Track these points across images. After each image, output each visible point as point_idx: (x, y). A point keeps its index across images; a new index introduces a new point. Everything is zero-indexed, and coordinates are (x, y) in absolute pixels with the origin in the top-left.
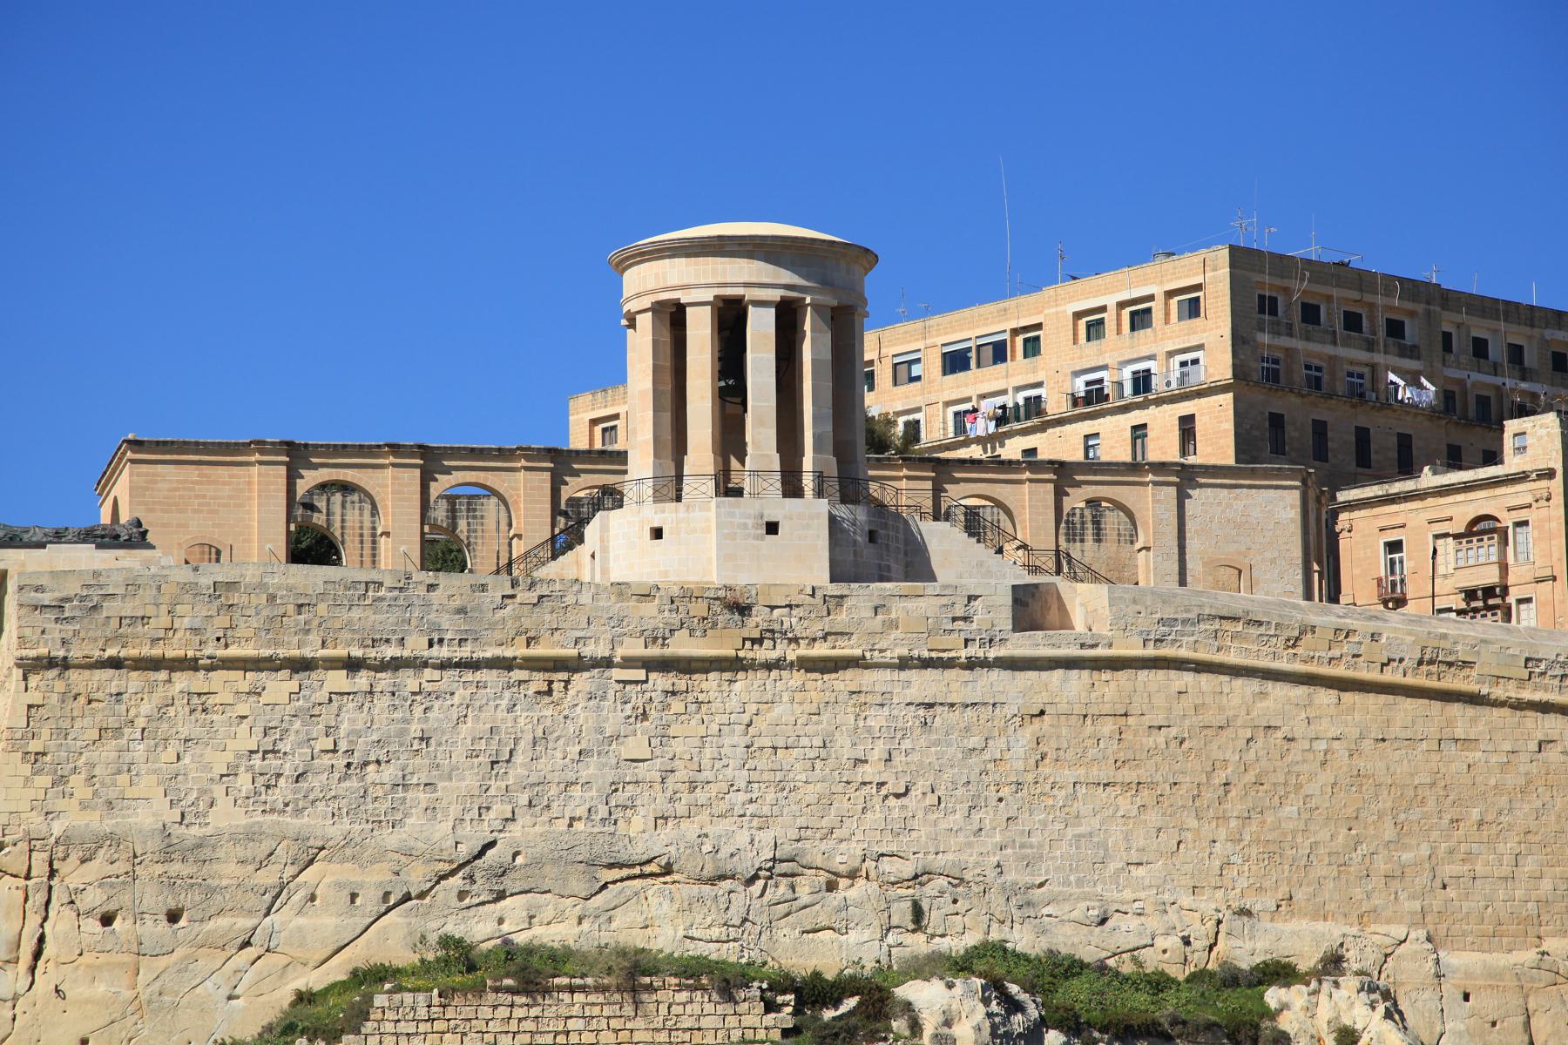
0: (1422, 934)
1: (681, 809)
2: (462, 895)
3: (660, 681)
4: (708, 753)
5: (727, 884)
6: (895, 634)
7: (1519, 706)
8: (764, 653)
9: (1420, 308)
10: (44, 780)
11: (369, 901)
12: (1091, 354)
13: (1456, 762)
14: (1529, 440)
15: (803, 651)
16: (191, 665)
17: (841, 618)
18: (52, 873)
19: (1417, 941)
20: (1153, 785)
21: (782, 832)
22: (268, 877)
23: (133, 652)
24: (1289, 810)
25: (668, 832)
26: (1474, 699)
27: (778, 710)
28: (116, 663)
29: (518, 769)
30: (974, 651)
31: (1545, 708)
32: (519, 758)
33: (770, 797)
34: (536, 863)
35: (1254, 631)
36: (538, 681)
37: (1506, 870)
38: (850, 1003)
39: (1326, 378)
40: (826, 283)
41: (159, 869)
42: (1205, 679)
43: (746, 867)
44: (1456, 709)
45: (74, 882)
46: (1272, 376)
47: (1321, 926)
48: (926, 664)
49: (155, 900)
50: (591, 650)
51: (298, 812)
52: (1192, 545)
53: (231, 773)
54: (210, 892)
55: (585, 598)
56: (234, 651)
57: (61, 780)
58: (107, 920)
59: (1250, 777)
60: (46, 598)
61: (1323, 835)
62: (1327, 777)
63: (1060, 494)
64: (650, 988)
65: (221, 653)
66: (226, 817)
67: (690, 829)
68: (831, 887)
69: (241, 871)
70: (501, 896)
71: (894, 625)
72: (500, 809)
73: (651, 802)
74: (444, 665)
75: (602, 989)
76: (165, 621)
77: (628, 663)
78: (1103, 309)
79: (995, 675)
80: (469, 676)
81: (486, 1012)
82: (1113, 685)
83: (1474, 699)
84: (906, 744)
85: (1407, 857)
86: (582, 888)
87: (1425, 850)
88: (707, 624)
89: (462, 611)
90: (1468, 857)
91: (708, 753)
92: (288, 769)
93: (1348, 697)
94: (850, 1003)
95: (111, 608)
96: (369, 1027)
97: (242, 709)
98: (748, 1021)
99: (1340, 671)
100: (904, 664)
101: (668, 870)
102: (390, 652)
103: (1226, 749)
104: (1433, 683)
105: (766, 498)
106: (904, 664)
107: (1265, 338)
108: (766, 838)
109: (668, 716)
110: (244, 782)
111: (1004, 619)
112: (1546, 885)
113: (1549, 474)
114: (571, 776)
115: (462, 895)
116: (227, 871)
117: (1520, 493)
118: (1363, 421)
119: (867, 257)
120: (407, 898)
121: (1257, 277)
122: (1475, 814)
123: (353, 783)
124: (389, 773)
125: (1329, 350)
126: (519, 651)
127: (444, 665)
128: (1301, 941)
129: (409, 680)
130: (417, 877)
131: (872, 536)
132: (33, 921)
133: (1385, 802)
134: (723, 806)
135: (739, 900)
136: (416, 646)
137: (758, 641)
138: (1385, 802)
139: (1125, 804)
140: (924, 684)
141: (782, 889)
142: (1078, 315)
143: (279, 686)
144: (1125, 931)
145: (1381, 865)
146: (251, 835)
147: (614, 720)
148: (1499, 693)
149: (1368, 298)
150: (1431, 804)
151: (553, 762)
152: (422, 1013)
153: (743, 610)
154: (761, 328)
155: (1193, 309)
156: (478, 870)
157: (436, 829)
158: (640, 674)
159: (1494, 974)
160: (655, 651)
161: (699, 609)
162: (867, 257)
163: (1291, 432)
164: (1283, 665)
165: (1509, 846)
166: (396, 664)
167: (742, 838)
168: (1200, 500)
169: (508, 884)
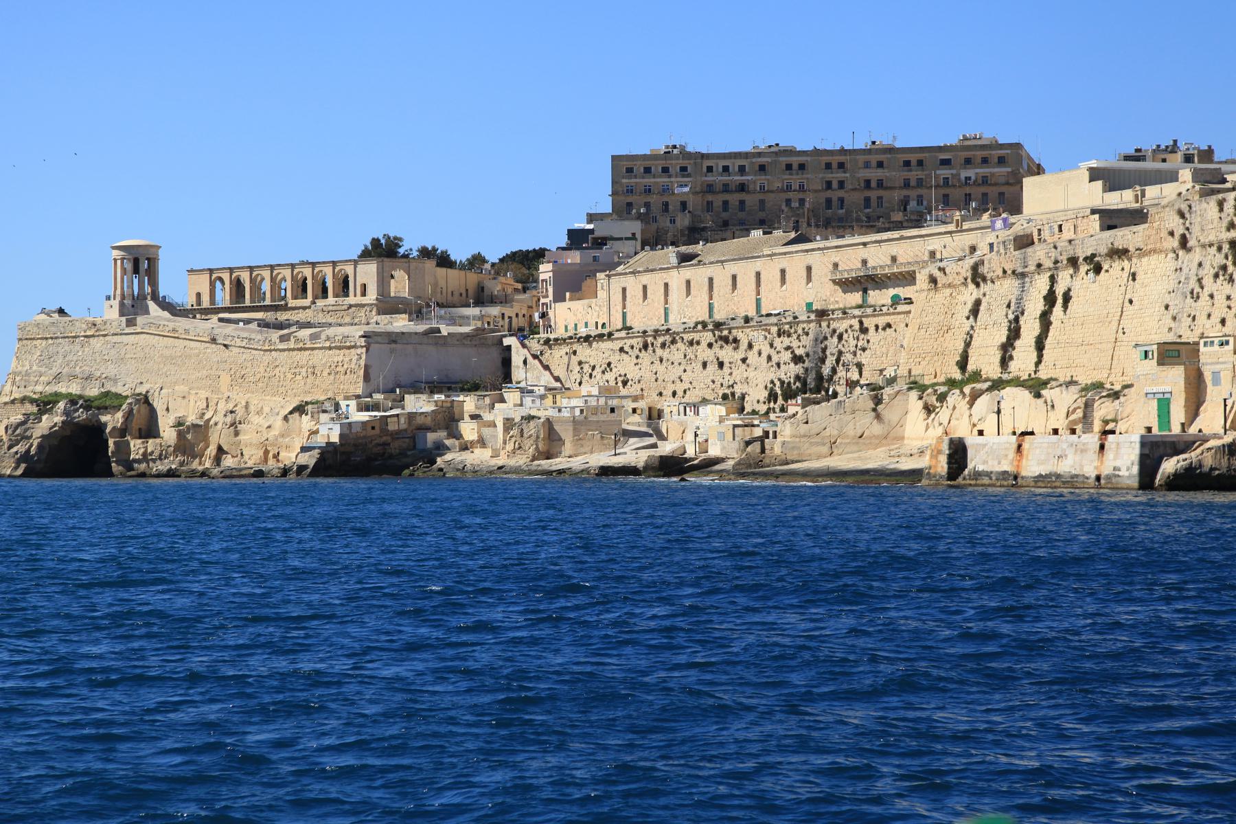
49: (23, 383)
143: (44, 342)
157: (55, 371)
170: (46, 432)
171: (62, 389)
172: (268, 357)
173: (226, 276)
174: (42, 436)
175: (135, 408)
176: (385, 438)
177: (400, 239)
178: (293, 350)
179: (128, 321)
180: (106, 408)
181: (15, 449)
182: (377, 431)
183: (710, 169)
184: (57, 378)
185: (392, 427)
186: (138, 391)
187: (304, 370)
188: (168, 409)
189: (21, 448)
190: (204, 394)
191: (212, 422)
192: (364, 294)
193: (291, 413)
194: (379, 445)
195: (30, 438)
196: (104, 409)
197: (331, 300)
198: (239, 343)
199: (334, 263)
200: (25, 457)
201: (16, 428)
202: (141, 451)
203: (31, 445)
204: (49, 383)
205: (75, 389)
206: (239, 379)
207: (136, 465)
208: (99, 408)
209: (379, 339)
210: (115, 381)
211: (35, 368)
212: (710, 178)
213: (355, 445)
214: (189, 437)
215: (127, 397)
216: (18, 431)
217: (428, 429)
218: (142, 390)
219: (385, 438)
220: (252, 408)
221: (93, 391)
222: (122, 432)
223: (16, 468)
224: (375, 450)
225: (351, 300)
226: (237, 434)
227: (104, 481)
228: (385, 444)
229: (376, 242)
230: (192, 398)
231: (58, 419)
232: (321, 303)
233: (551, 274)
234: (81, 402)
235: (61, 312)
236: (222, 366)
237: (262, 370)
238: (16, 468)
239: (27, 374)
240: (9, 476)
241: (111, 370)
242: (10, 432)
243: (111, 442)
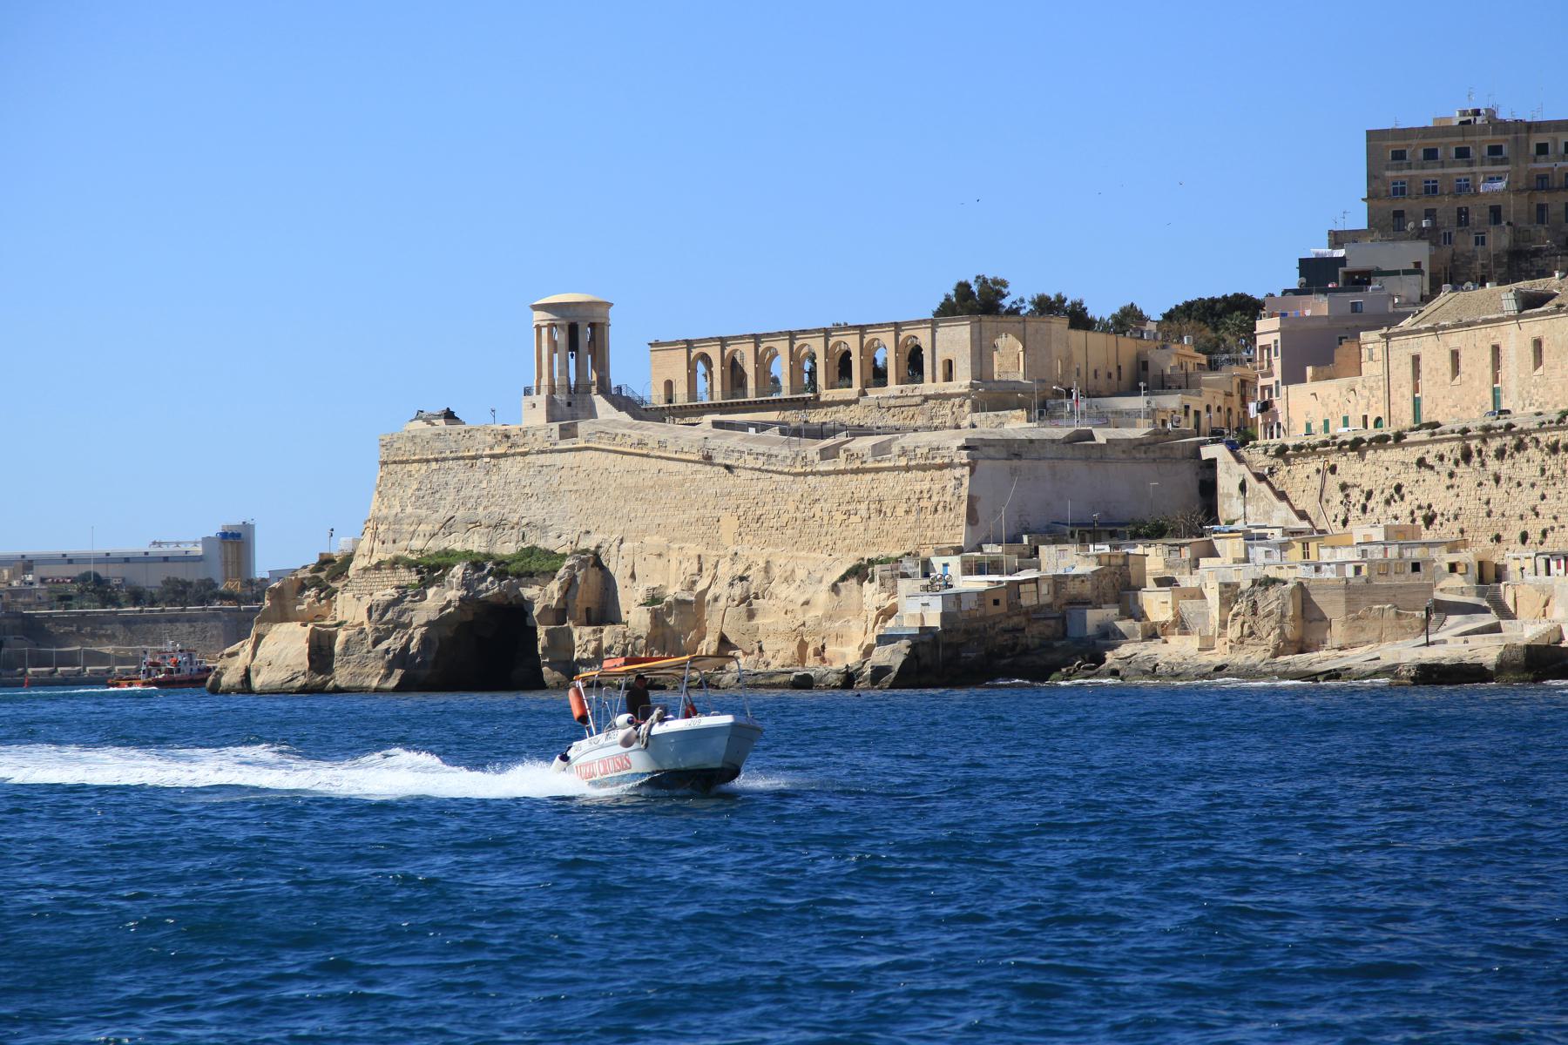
9: (1510, 137)
16: (406, 462)
40: (563, 317)
49: (391, 536)
52: (938, 351)
79: (556, 455)
83: (647, 456)
95: (396, 445)
121: (1385, 143)
125: (1439, 171)
131: (569, 404)
140: (543, 459)
143: (424, 467)
157: (443, 514)
170: (434, 616)
171: (456, 544)
172: (801, 485)
173: (714, 353)
174: (429, 623)
175: (580, 574)
176: (1016, 619)
177: (1004, 284)
178: (844, 472)
179: (562, 428)
180: (531, 575)
182: (1003, 608)
183: (1542, 149)
184: (448, 525)
185: (1027, 600)
186: (582, 546)
187: (863, 506)
188: (633, 576)
189: (394, 643)
190: (693, 549)
191: (709, 597)
192: (949, 377)
193: (843, 578)
194: (1006, 631)
195: (408, 625)
196: (528, 576)
197: (893, 388)
198: (751, 462)
199: (897, 327)
200: (401, 658)
201: (385, 611)
203: (411, 639)
204: (433, 535)
205: (476, 543)
206: (752, 523)
208: (518, 576)
209: (991, 451)
210: (544, 529)
211: (409, 510)
212: (1543, 165)
213: (967, 632)
214: (671, 621)
215: (564, 556)
216: (389, 616)
217: (1086, 603)
218: (589, 543)
219: (1016, 619)
220: (776, 571)
221: (507, 547)
222: (560, 614)
223: (387, 677)
224: (1000, 640)
225: (927, 387)
226: (751, 615)
227: (530, 699)
228: (1017, 630)
229: (963, 289)
230: (674, 556)
231: (454, 594)
232: (874, 393)
233: (1277, 336)
234: (489, 565)
235: (449, 416)
236: (723, 502)
237: (791, 507)
239: (397, 520)
240: (377, 690)
241: (536, 512)
242: (375, 616)
243: (541, 632)
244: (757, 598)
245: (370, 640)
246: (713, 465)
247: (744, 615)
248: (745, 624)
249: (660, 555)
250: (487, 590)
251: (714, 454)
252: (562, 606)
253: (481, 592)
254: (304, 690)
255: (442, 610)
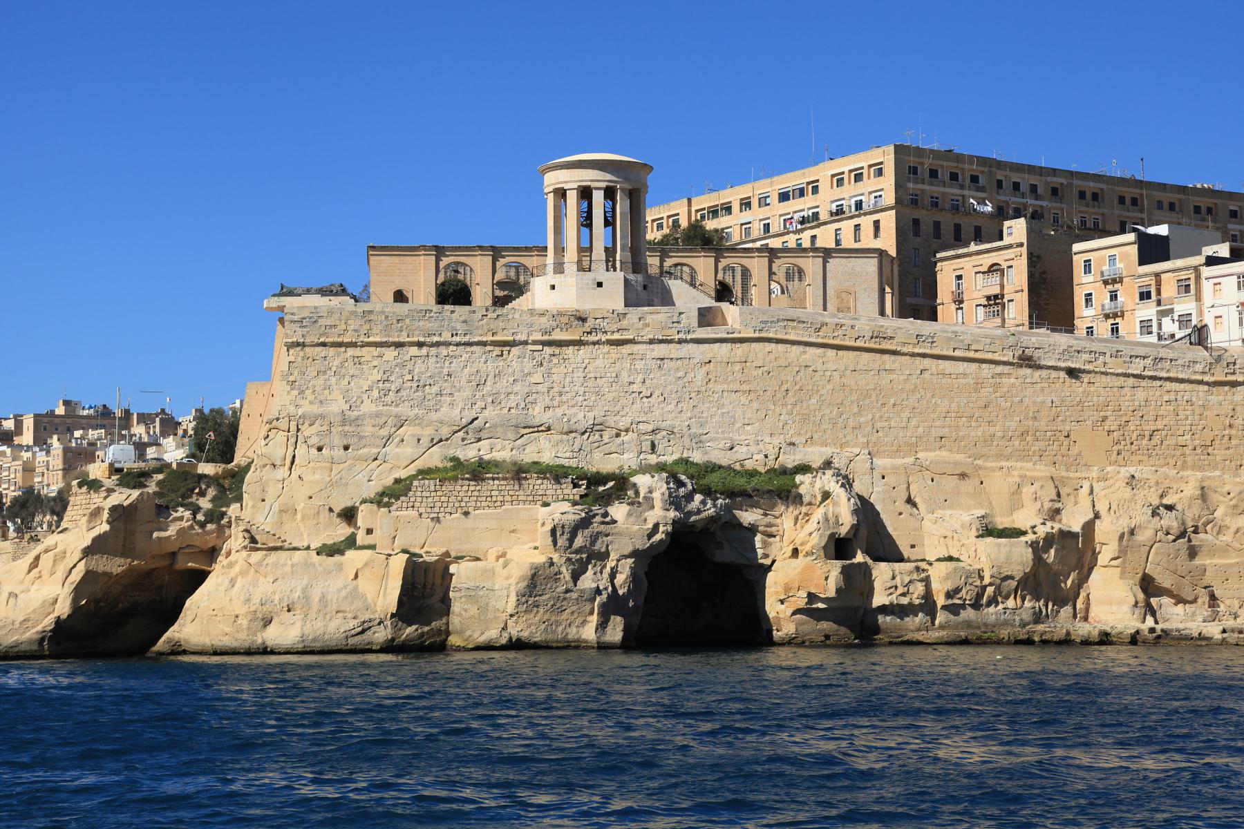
0: (866, 451)
1: (556, 403)
2: (463, 439)
3: (548, 350)
4: (568, 380)
5: (573, 435)
6: (648, 329)
7: (913, 355)
8: (593, 338)
9: (986, 169)
10: (295, 392)
11: (425, 442)
12: (838, 193)
13: (885, 379)
14: (1014, 230)
15: (609, 337)
16: (353, 345)
17: (625, 323)
18: (298, 430)
19: (864, 456)
20: (756, 391)
21: (598, 413)
22: (384, 432)
23: (331, 340)
24: (813, 401)
25: (550, 413)
26: (894, 353)
27: (598, 362)
28: (324, 344)
29: (488, 388)
30: (682, 336)
31: (924, 356)
32: (488, 383)
33: (593, 398)
34: (494, 426)
35: (801, 326)
36: (497, 350)
37: (904, 424)
38: (611, 484)
39: (940, 202)
41: (340, 429)
42: (780, 347)
43: (581, 428)
44: (886, 357)
45: (307, 434)
46: (914, 202)
47: (824, 449)
48: (661, 341)
49: (338, 441)
50: (519, 337)
51: (397, 405)
53: (370, 389)
54: (361, 438)
55: (517, 316)
56: (371, 339)
57: (302, 392)
58: (320, 449)
59: (797, 387)
60: (296, 318)
61: (828, 411)
62: (830, 387)
63: (771, 262)
64: (526, 478)
65: (367, 340)
66: (368, 407)
67: (559, 412)
68: (618, 435)
69: (373, 429)
70: (479, 440)
71: (647, 325)
72: (480, 404)
73: (543, 401)
74: (458, 344)
75: (505, 479)
76: (343, 327)
77: (535, 343)
78: (843, 173)
79: (690, 346)
80: (468, 349)
81: (458, 488)
82: (740, 349)
83: (894, 353)
84: (652, 376)
85: (862, 419)
86: (513, 437)
87: (870, 417)
88: (568, 326)
89: (465, 322)
90: (888, 419)
91: (568, 380)
92: (393, 388)
93: (841, 353)
94: (611, 484)
95: (322, 322)
96: (411, 494)
97: (375, 363)
98: (566, 491)
99: (837, 342)
100: (651, 342)
101: (549, 429)
102: (435, 339)
103: (788, 375)
104: (877, 346)
105: (600, 272)
106: (651, 342)
107: (911, 185)
108: (591, 415)
109: (551, 365)
110: (375, 393)
111: (694, 322)
112: (920, 430)
113: (1021, 245)
114: (510, 390)
115: (463, 439)
116: (368, 430)
117: (1009, 254)
118: (957, 221)
119: (647, 168)
120: (441, 441)
121: (907, 158)
122: (892, 401)
123: (420, 394)
124: (435, 389)
125: (942, 189)
126: (490, 338)
127: (458, 344)
128: (815, 455)
129: (444, 351)
130: (445, 432)
131: (645, 287)
132: (291, 449)
133: (854, 396)
134: (573, 402)
135: (578, 441)
136: (446, 336)
137: (590, 333)
138: (854, 396)
139: (744, 400)
140: (660, 350)
141: (597, 437)
142: (833, 176)
143: (390, 353)
144: (741, 452)
145: (851, 423)
146: (378, 415)
147: (528, 366)
148: (905, 350)
149: (961, 165)
150: (874, 397)
151: (502, 384)
152: (432, 488)
153: (583, 320)
154: (598, 197)
155: (880, 173)
156: (470, 429)
157: (453, 412)
158: (540, 347)
159: (895, 468)
160: (546, 338)
161: (565, 319)
162: (647, 168)
163: (923, 226)
164: (813, 340)
165: (907, 414)
166: (438, 344)
167: (581, 416)
168: (833, 263)
169: (482, 435)
170: (643, 544)
174: (635, 554)
181: (587, 581)
188: (910, 501)
195: (604, 556)
202: (919, 589)
207: (881, 618)
216: (579, 541)
226: (1193, 553)
231: (660, 515)
238: (602, 626)
242: (562, 541)
244: (1196, 532)
245: (566, 574)
246: (1040, 367)
247: (1184, 553)
248: (1183, 564)
249: (963, 476)
250: (699, 512)
251: (1037, 354)
252: (851, 536)
253: (690, 513)
254: (390, 647)
255: (650, 536)
